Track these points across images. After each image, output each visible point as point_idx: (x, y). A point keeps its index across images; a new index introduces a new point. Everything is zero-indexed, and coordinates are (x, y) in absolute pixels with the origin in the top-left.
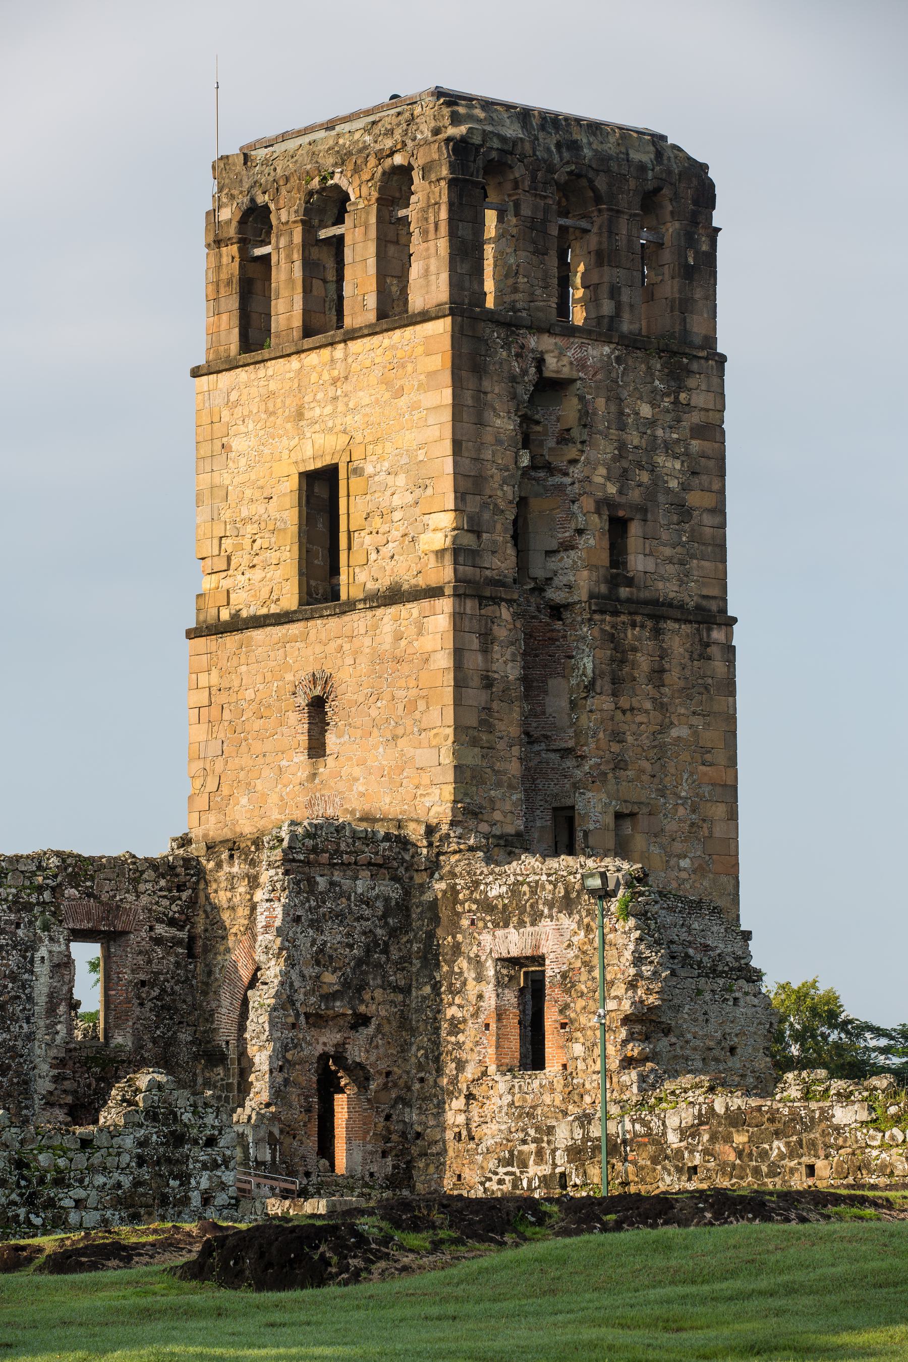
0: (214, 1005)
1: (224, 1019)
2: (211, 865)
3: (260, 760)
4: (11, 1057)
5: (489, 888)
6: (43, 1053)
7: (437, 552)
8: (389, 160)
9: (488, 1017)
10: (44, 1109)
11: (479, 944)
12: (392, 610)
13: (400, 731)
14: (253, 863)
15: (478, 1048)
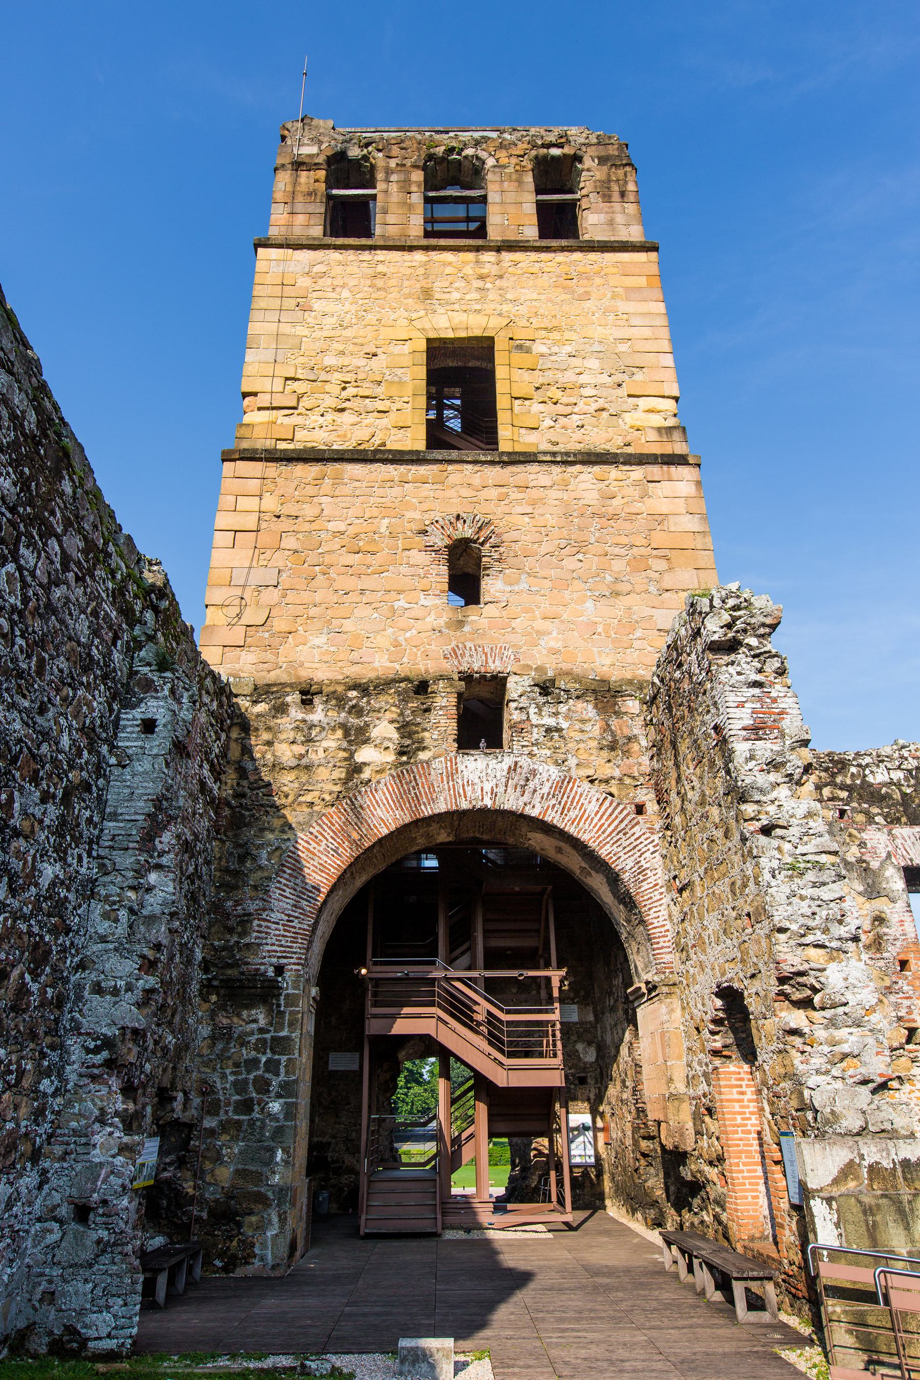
0: (252, 907)
1: (273, 929)
2: (261, 707)
3: (353, 597)
4: (55, 931)
5: (867, 772)
6: (121, 930)
7: (659, 430)
8: (545, 151)
9: (906, 949)
10: (94, 1078)
11: (863, 844)
12: (596, 469)
13: (624, 587)
14: (357, 711)
15: (893, 998)
